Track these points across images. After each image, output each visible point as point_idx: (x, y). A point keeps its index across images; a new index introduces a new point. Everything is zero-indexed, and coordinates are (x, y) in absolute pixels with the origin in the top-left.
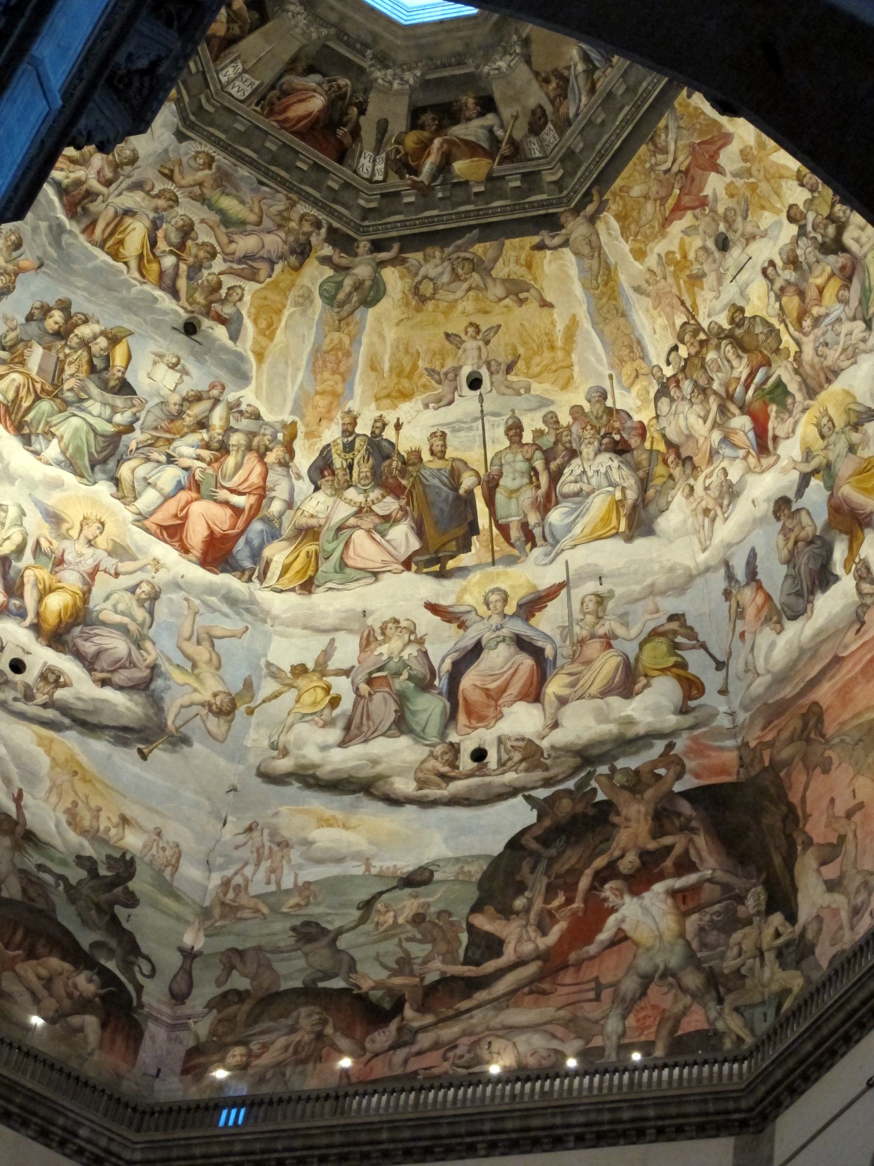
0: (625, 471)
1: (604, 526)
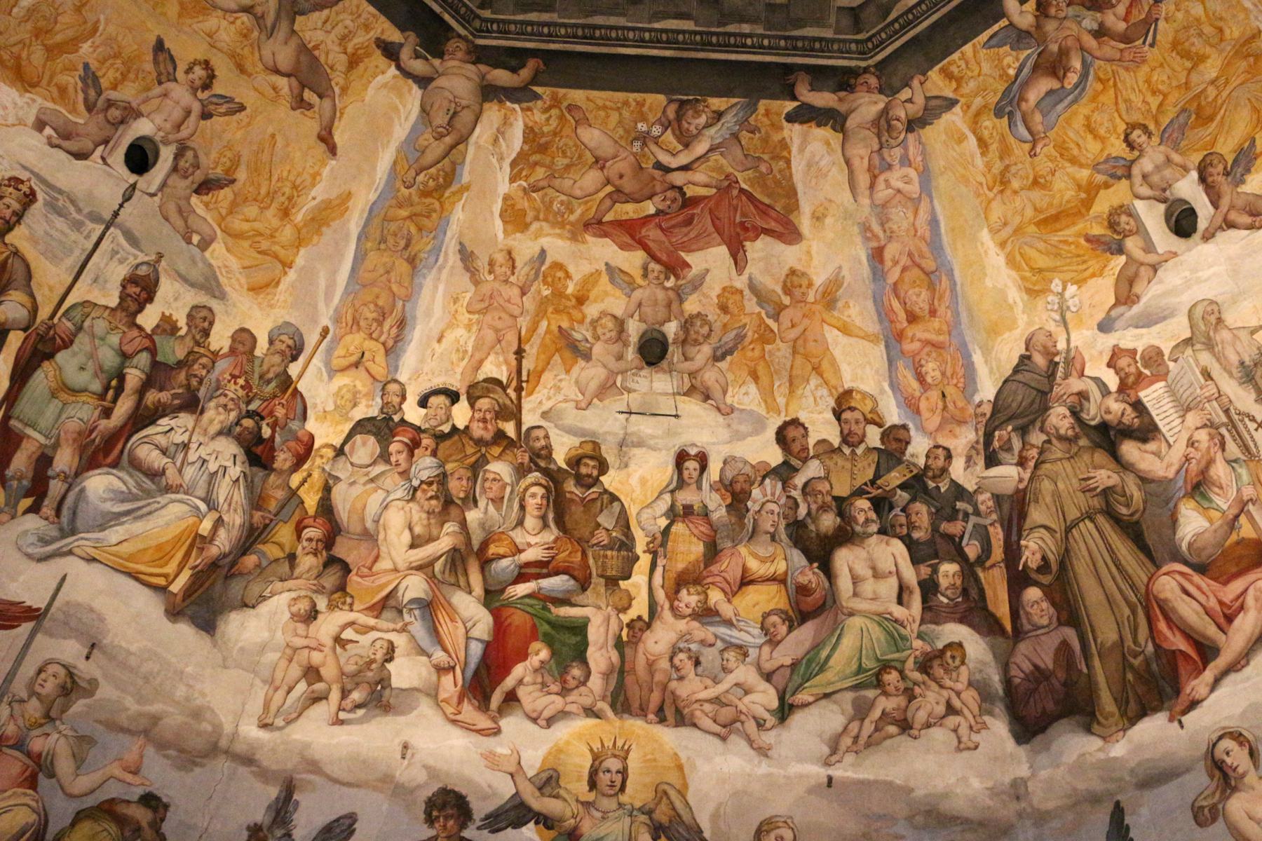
0: (240, 496)
1: (152, 562)
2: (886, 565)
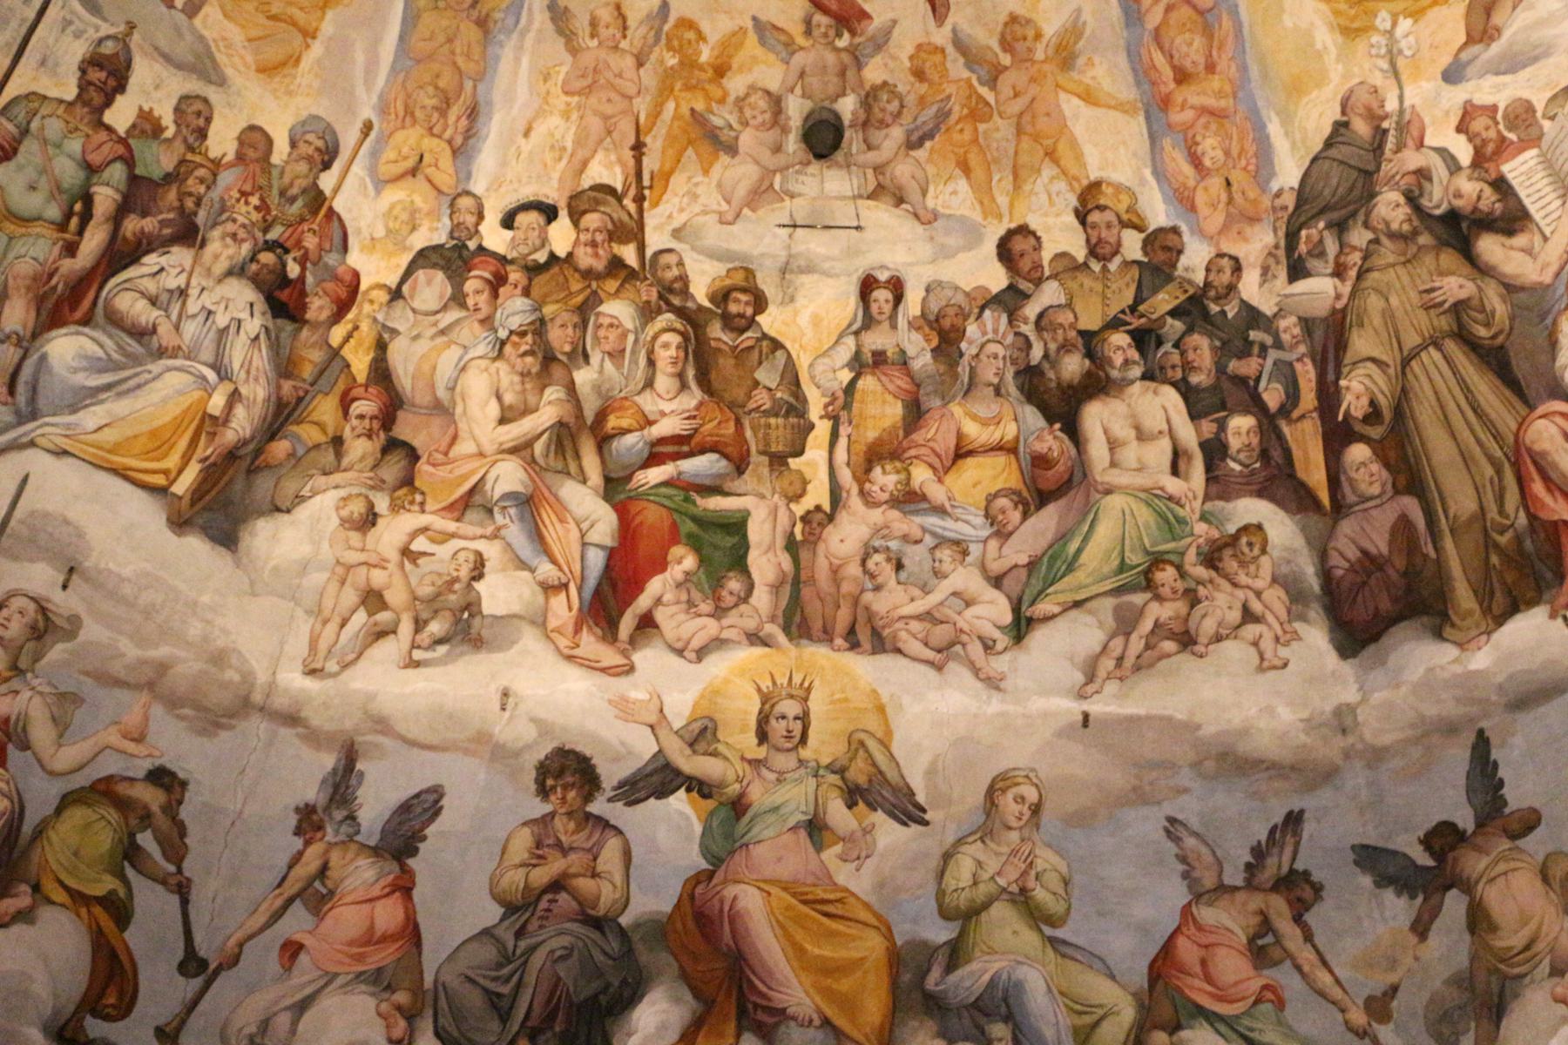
0: (261, 360)
1: (146, 454)
2: (1154, 422)
